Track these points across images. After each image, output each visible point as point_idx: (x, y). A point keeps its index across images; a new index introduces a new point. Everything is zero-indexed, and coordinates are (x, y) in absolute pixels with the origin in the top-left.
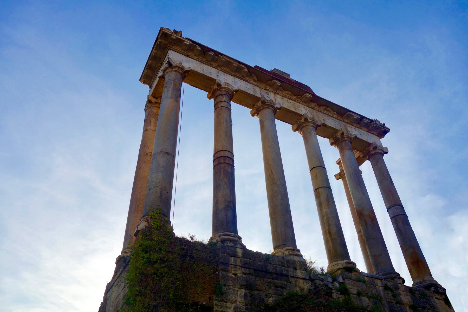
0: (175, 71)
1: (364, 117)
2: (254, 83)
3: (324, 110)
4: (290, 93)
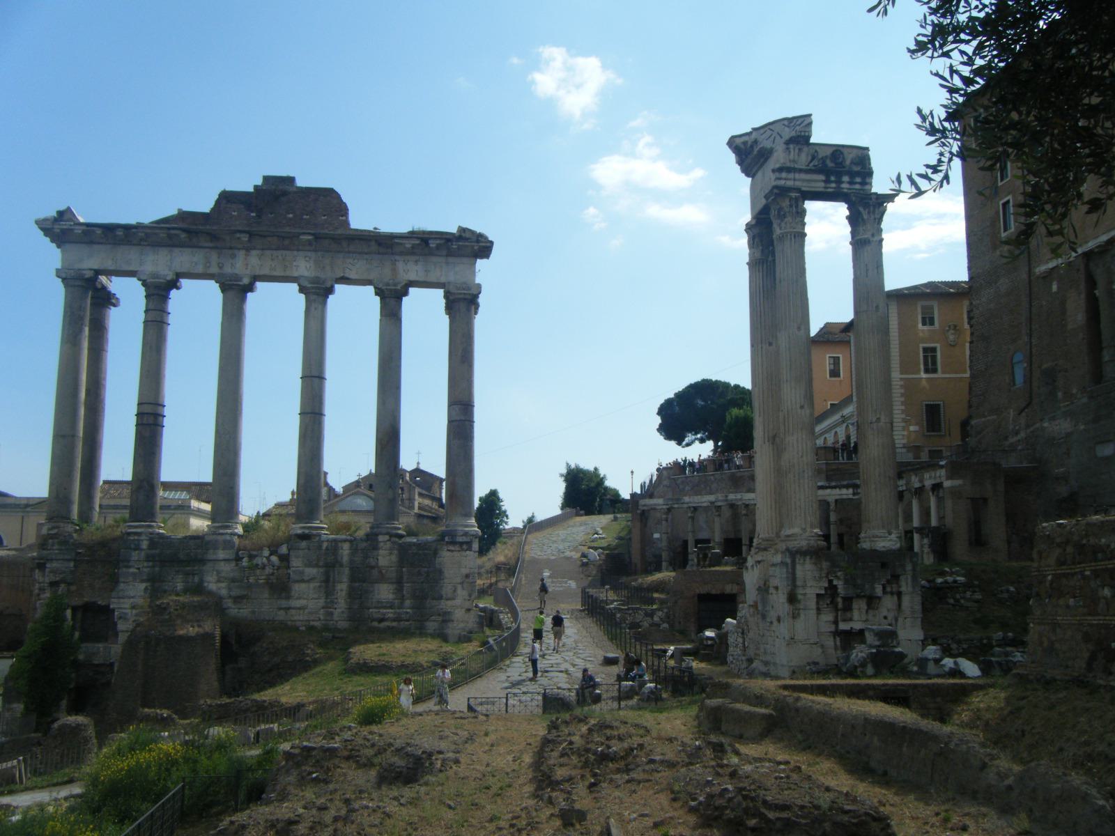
0: (72, 286)
1: (430, 239)
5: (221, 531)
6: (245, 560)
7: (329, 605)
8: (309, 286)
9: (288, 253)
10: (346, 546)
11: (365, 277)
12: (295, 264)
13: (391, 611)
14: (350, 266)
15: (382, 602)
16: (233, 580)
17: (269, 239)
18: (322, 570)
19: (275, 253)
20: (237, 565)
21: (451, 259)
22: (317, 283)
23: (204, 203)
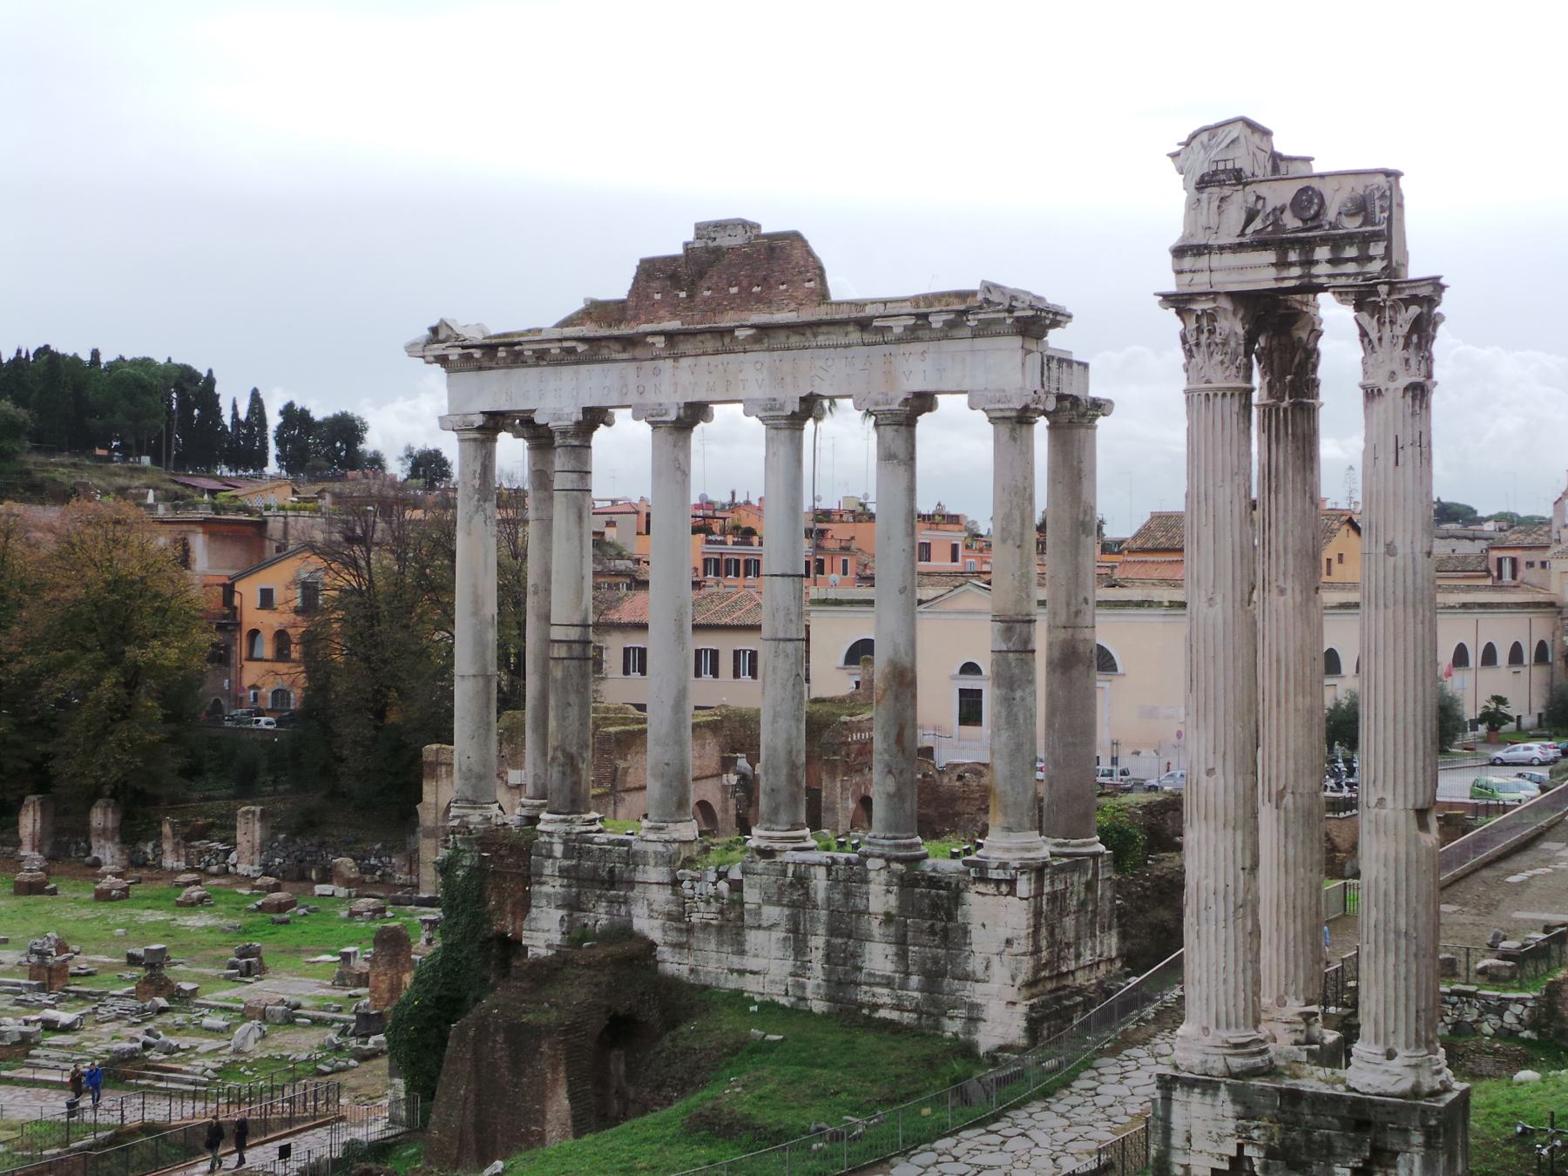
3: (815, 335)
4: (708, 336)
5: (651, 836)
6: (686, 884)
7: (801, 969)
9: (732, 356)
10: (821, 872)
12: (741, 376)
13: (886, 991)
15: (873, 975)
16: (670, 916)
17: (700, 338)
18: (787, 911)
20: (675, 893)
23: (618, 288)
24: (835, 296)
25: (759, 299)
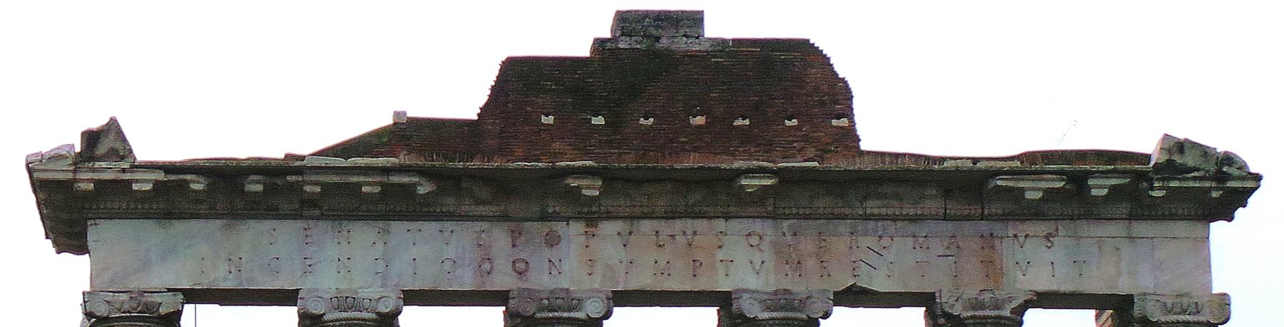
1: (1089, 174)
2: (481, 210)
3: (865, 199)
4: (669, 186)
8: (766, 315)
9: (701, 224)
11: (914, 287)
12: (720, 255)
14: (872, 258)
19: (665, 227)
21: (1141, 228)
22: (782, 309)
24: (869, 142)
25: (746, 137)
